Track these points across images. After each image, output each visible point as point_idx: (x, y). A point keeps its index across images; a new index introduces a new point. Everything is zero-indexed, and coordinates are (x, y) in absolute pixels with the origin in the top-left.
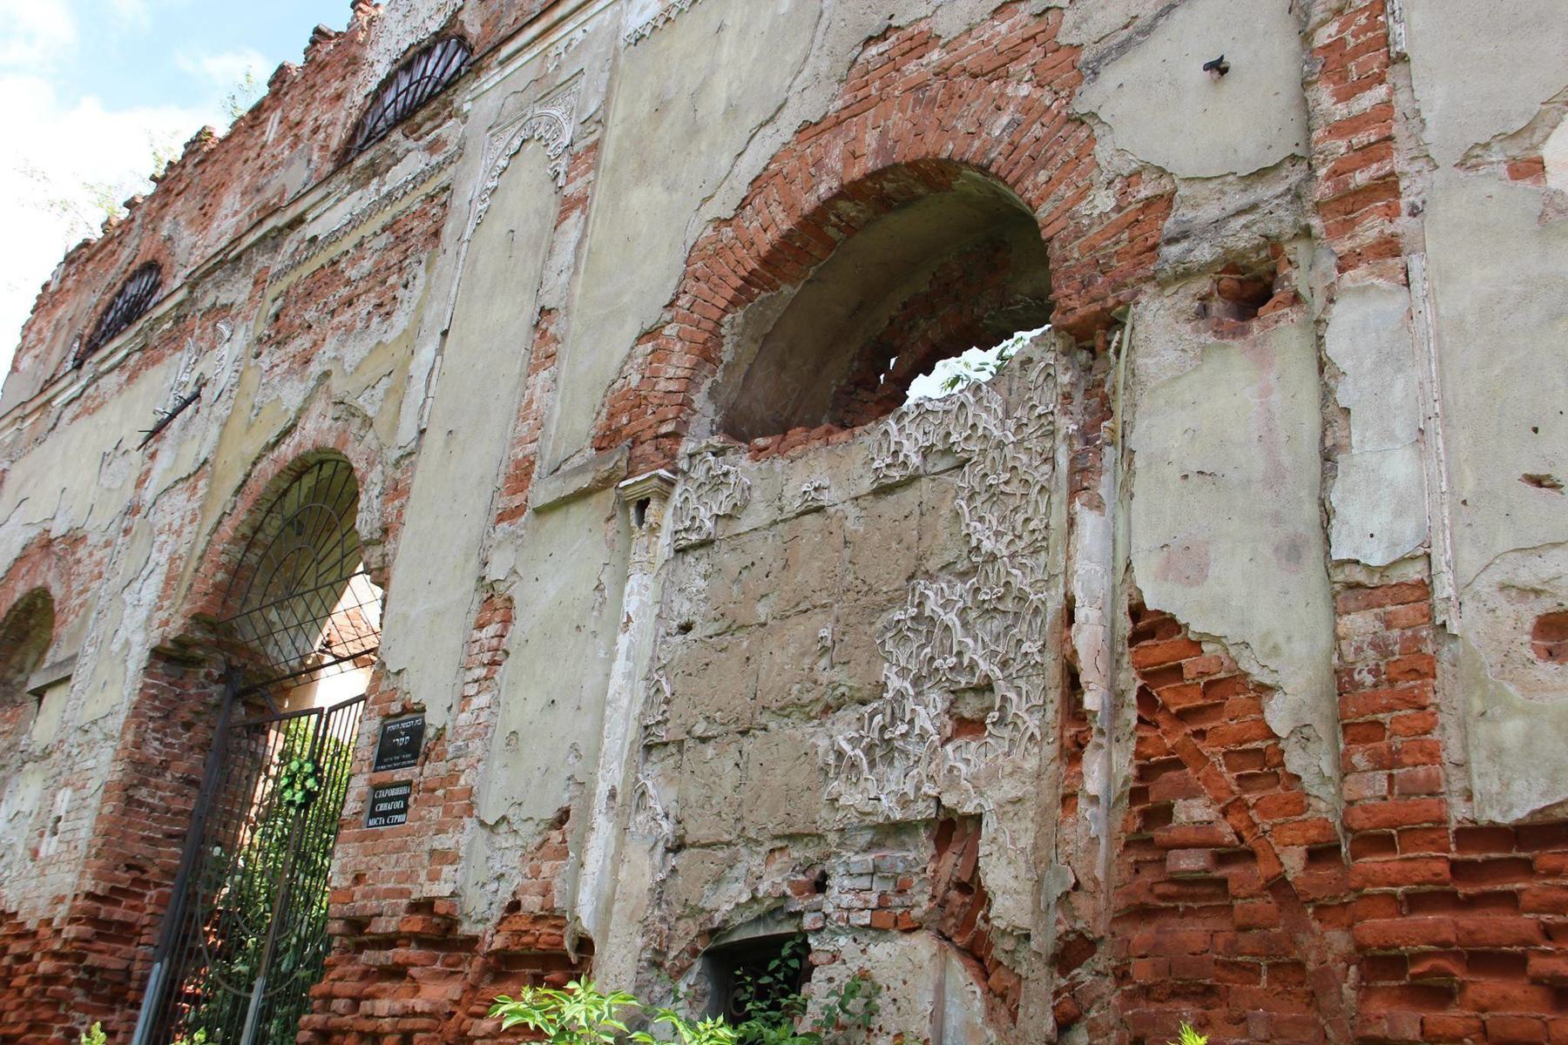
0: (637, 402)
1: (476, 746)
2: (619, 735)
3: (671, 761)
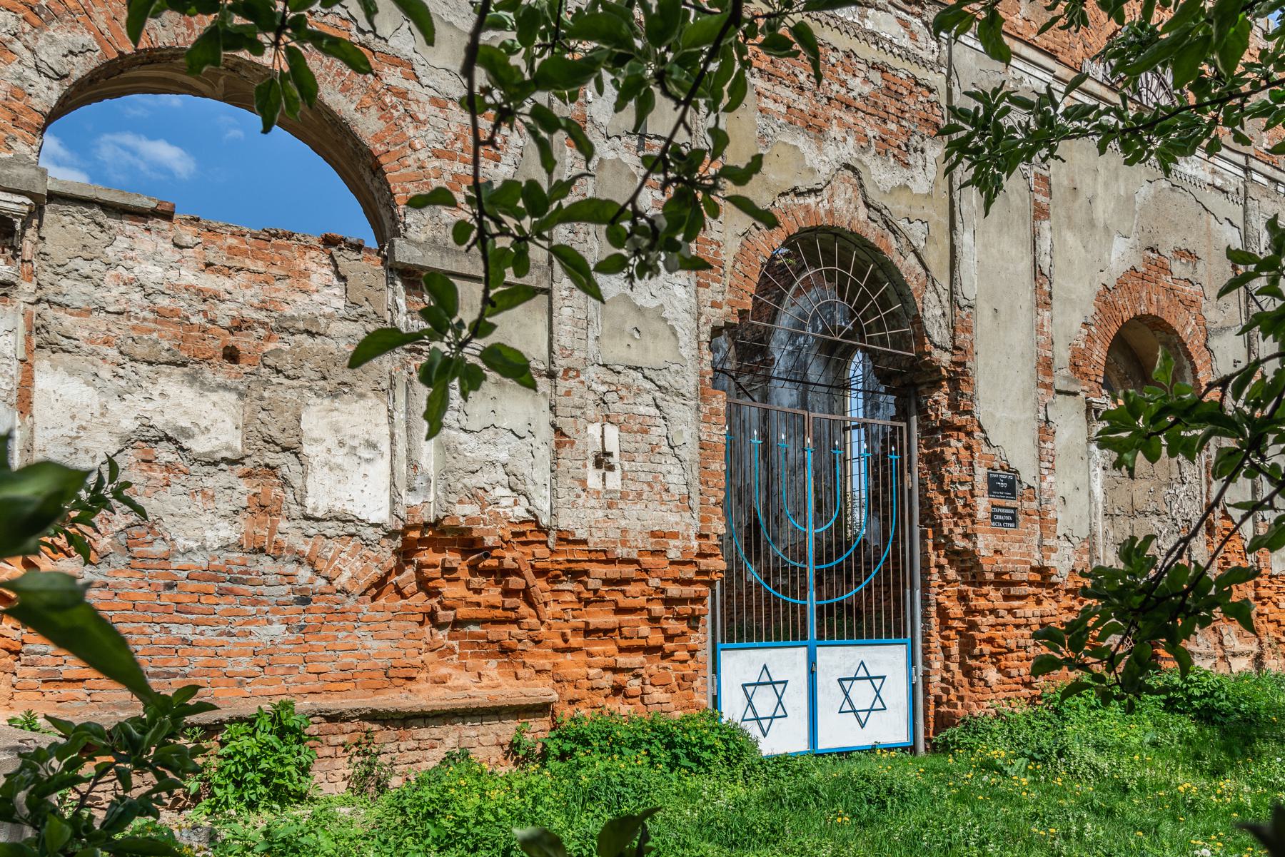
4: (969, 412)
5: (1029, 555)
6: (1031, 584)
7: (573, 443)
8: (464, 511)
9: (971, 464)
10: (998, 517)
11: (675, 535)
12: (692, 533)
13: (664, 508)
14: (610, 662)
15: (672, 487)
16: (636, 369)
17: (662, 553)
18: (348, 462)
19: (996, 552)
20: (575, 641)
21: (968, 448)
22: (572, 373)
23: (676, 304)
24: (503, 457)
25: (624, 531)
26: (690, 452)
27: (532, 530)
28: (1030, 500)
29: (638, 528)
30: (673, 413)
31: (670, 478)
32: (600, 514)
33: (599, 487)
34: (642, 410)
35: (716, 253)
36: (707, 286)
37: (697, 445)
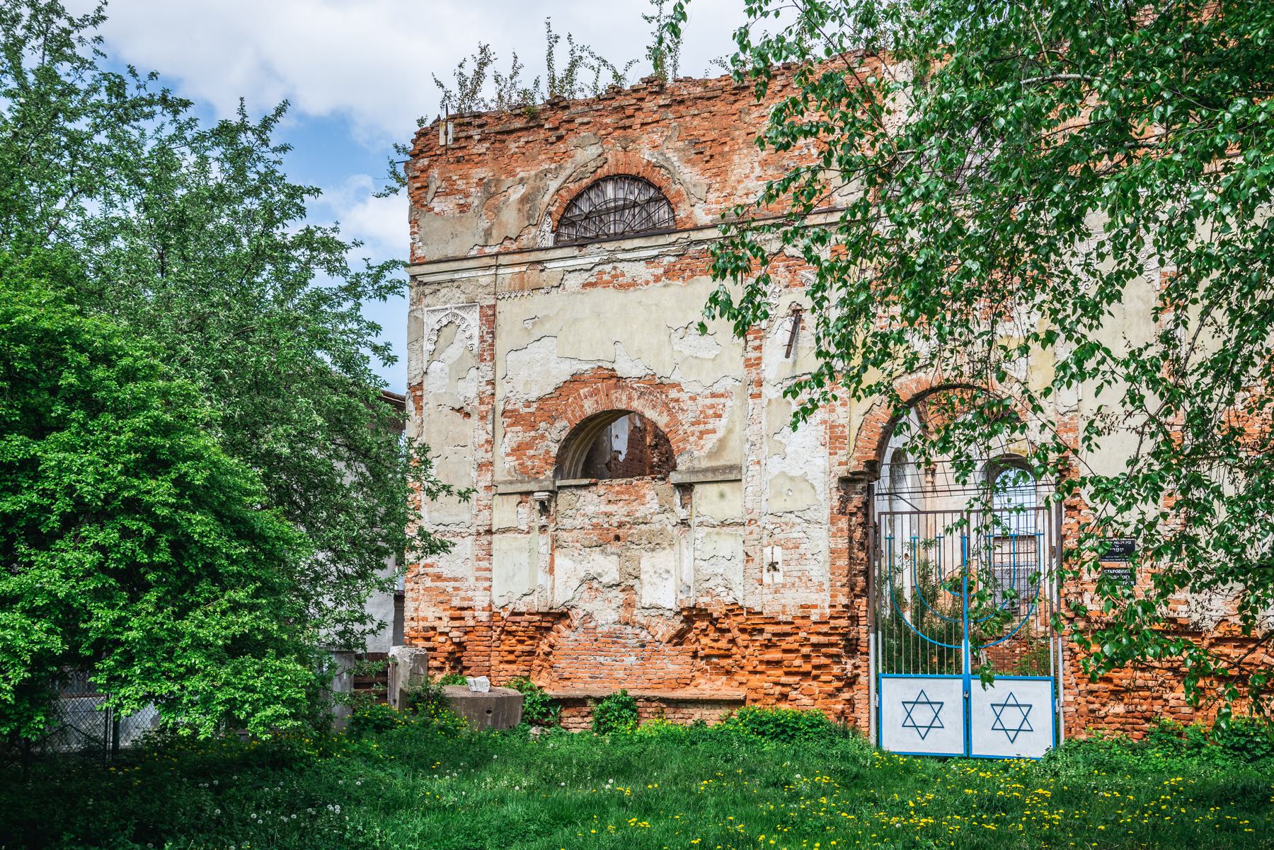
8: (703, 601)
11: (815, 607)
12: (827, 605)
14: (776, 679)
18: (658, 581)
20: (760, 668)
24: (721, 571)
26: (825, 556)
27: (734, 610)
32: (770, 597)
34: (795, 535)
35: (843, 432)
37: (828, 551)
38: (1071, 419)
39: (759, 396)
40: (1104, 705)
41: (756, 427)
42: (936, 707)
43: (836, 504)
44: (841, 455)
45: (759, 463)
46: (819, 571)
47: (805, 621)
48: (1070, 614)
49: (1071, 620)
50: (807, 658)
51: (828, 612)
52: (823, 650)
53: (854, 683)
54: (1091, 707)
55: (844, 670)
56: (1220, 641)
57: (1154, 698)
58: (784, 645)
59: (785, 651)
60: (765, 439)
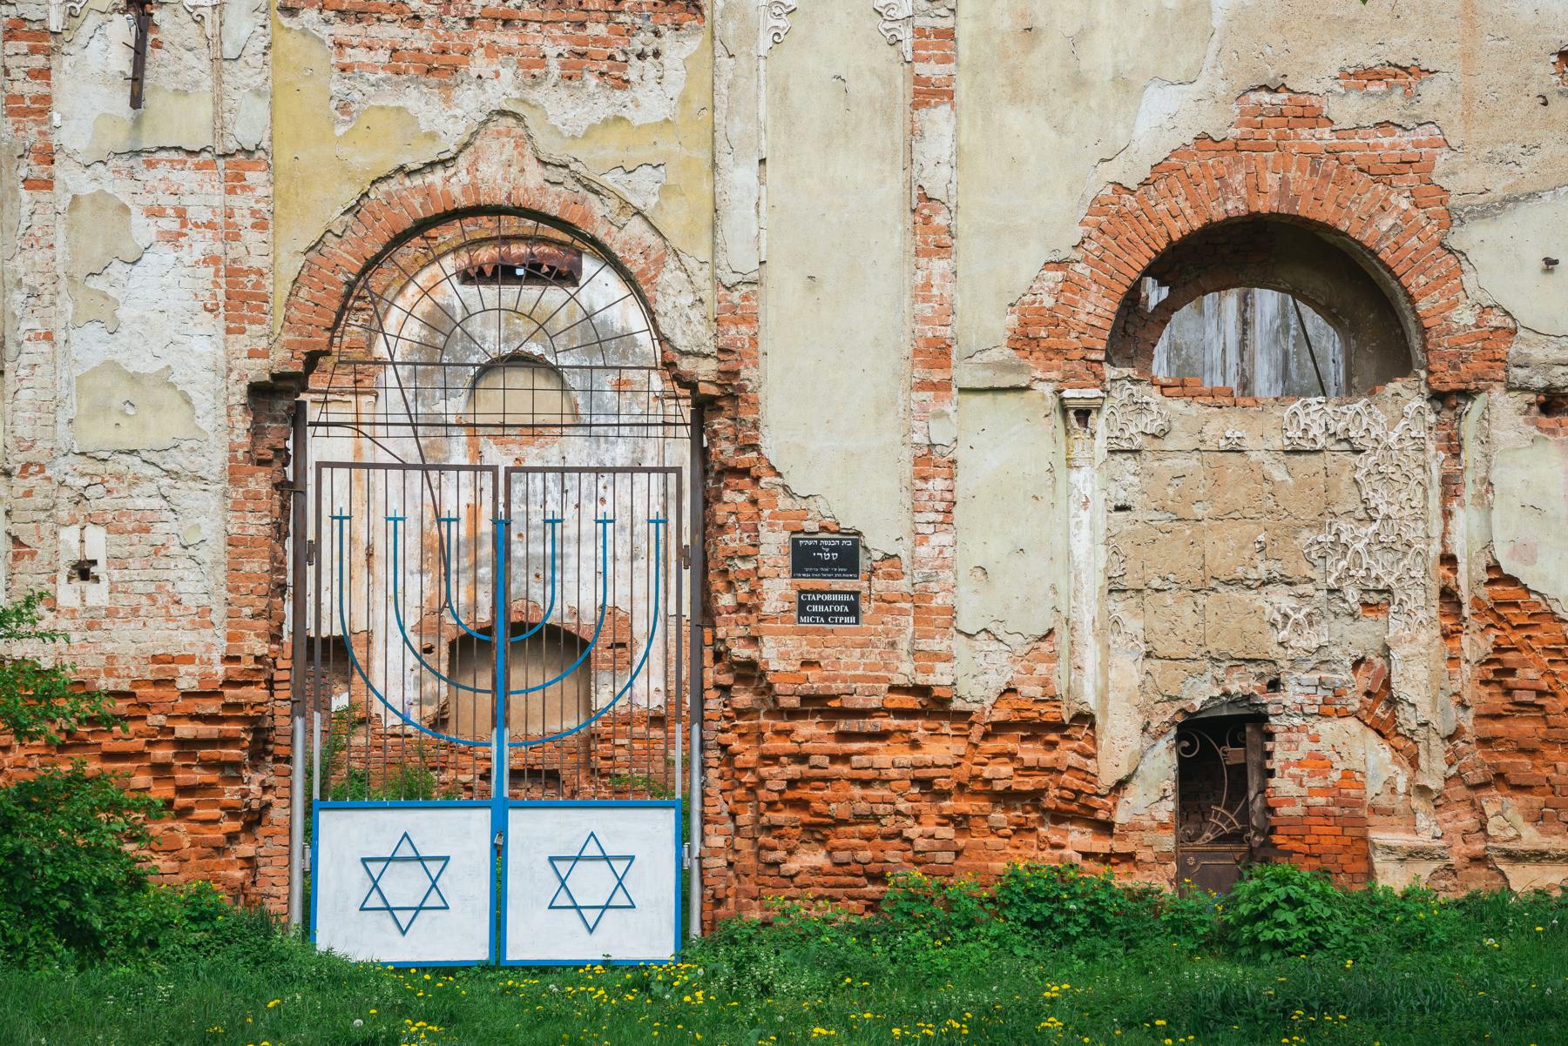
0: (1053, 321)
1: (946, 575)
2: (1092, 583)
3: (1133, 602)
4: (754, 447)
5: (886, 666)
6: (900, 713)
7: (33, 554)
9: (756, 530)
10: (815, 608)
11: (190, 659)
12: (216, 656)
13: (172, 625)
15: (184, 598)
16: (131, 452)
17: (171, 682)
19: (806, 664)
21: (754, 502)
22: (33, 469)
23: (192, 362)
25: (111, 658)
26: (214, 550)
28: (890, 576)
29: (132, 653)
30: (187, 503)
31: (181, 586)
33: (77, 604)
35: (257, 285)
36: (242, 331)
37: (222, 542)
38: (746, 298)
39: (48, 184)
40: (790, 852)
41: (39, 256)
42: (434, 868)
43: (242, 438)
44: (255, 337)
45: (48, 336)
46: (199, 583)
47: (161, 691)
48: (726, 679)
49: (725, 690)
50: (162, 770)
51: (220, 670)
52: (203, 753)
53: (259, 822)
54: (772, 856)
55: (245, 794)
56: (999, 728)
57: (886, 837)
58: (108, 743)
59: (109, 756)
60: (63, 284)
